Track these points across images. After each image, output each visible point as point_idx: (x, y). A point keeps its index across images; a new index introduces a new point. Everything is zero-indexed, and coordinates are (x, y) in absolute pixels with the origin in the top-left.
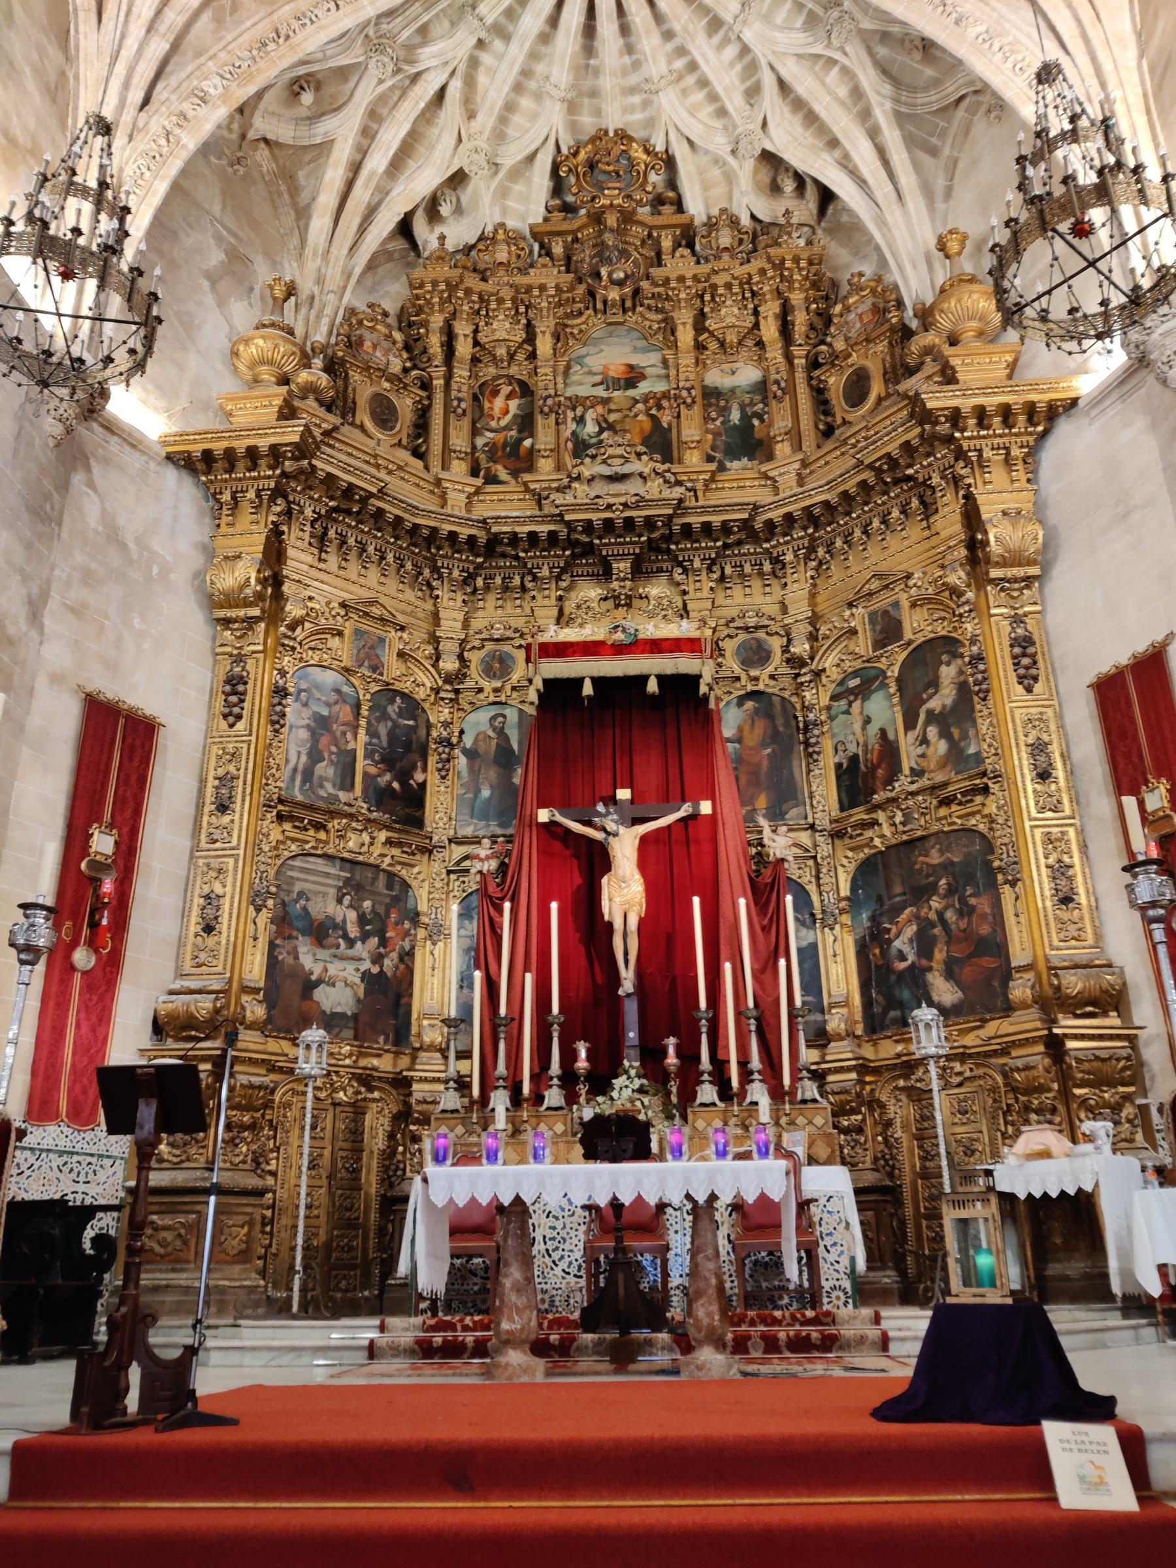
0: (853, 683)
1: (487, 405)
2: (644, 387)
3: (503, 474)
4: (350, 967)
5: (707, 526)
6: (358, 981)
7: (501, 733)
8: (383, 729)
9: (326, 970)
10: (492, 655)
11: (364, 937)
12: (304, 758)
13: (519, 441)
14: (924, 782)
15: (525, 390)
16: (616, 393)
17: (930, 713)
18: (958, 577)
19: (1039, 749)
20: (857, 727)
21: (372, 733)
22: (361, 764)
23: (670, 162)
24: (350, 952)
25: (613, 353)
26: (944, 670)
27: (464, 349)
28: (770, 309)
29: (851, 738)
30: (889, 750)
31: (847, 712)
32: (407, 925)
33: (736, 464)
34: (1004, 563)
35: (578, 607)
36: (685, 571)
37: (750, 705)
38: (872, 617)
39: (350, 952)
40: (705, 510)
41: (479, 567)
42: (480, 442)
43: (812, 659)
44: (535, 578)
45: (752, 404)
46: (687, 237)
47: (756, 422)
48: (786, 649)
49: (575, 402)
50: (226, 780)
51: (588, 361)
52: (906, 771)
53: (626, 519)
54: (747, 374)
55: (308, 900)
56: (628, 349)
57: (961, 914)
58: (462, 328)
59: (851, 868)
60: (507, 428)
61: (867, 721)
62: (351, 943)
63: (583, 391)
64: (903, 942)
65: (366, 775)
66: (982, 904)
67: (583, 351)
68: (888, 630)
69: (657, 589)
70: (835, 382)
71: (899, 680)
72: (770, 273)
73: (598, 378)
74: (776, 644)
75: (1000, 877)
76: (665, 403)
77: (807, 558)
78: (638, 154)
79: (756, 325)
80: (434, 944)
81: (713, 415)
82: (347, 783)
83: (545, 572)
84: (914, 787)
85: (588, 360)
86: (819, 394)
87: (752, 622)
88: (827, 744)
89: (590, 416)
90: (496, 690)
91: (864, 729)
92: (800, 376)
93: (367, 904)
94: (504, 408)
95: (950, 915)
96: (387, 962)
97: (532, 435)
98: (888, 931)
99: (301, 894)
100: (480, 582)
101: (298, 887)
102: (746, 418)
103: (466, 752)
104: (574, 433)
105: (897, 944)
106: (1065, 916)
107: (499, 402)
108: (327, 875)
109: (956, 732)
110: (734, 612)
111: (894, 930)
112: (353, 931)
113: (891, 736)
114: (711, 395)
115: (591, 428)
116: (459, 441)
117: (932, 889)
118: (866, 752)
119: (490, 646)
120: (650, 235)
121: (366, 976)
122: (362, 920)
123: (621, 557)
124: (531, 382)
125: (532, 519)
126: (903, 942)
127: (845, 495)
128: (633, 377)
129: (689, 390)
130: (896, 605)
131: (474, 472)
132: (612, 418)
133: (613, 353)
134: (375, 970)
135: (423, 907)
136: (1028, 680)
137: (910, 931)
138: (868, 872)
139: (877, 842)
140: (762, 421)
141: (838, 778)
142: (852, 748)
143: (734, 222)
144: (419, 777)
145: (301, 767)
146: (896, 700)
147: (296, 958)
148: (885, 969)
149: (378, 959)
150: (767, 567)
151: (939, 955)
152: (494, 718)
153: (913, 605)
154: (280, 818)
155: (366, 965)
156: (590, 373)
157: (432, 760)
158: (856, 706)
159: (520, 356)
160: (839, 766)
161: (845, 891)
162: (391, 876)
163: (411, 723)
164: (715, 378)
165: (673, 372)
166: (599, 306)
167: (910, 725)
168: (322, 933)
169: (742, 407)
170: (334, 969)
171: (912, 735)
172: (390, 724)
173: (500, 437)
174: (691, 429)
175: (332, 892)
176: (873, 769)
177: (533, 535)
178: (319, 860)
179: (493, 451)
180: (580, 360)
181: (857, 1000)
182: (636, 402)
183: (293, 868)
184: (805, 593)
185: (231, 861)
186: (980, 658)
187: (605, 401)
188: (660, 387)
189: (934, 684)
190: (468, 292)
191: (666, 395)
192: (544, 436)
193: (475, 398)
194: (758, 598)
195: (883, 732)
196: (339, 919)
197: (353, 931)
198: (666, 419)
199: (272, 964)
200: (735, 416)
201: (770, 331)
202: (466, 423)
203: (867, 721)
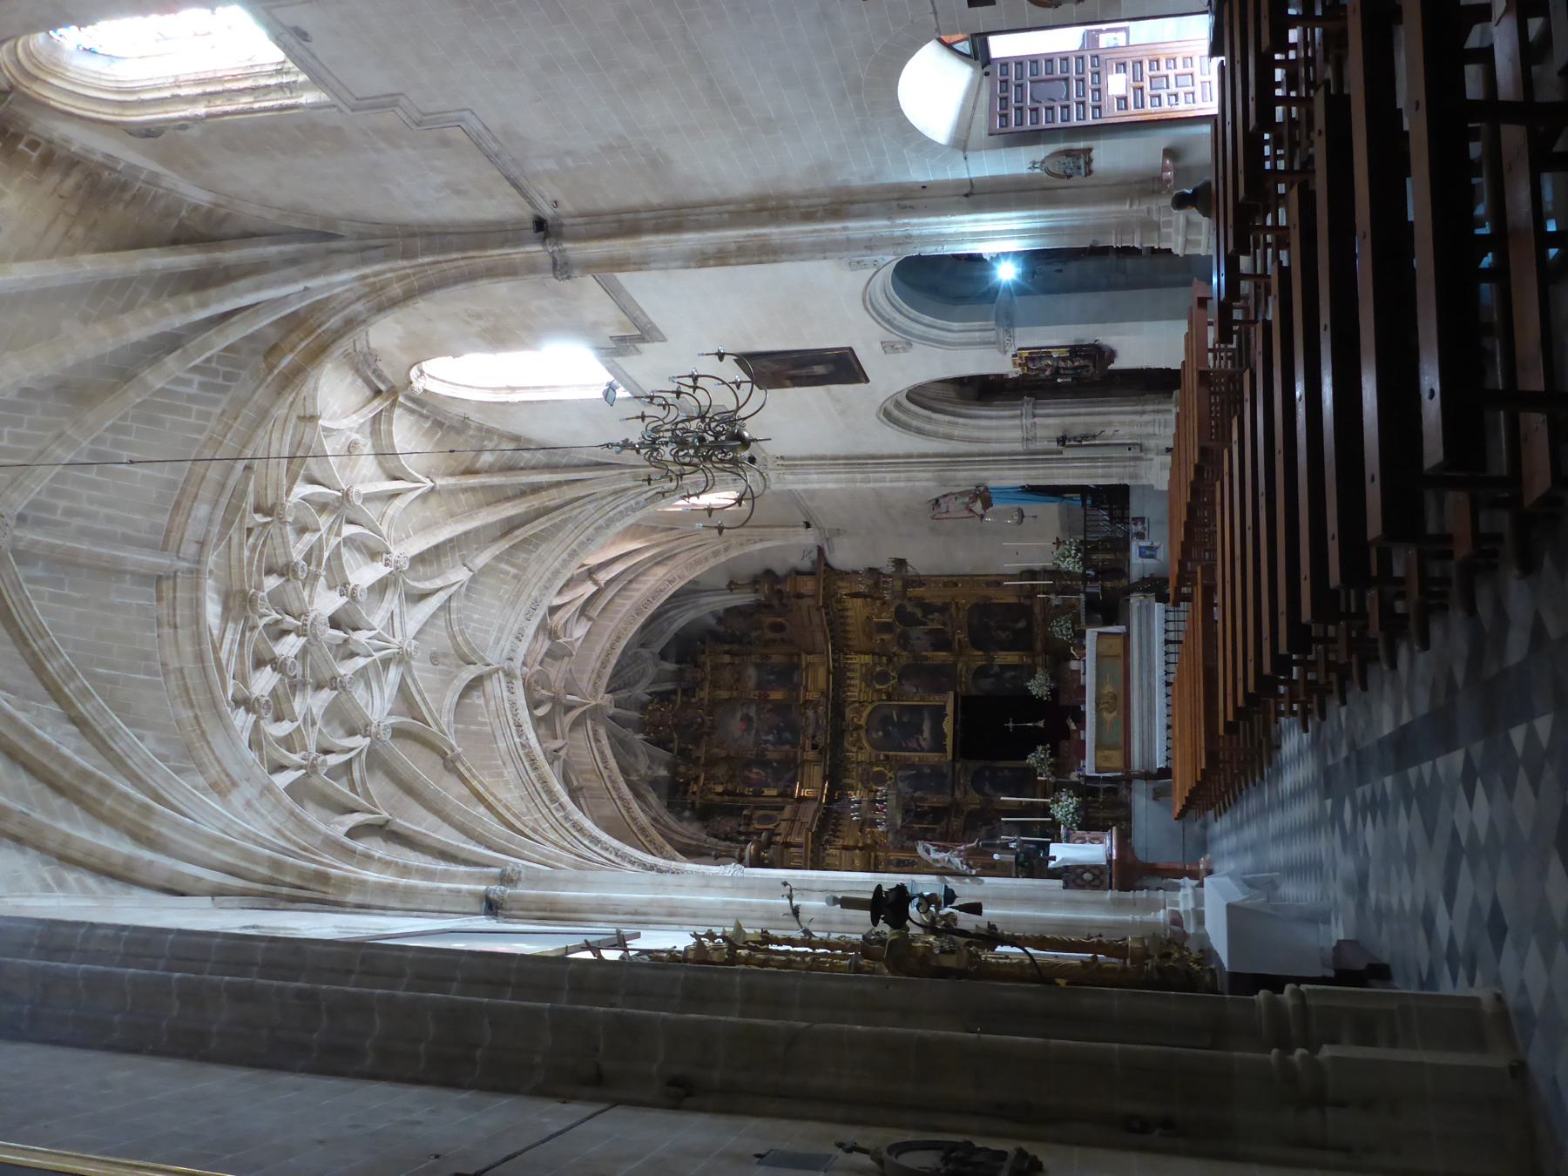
2: (752, 712)
15: (748, 765)
18: (878, 603)
25: (735, 725)
27: (730, 787)
28: (727, 659)
30: (931, 632)
33: (796, 679)
54: (751, 674)
58: (720, 789)
63: (751, 739)
64: (1003, 635)
68: (886, 628)
70: (770, 635)
94: (755, 773)
114: (761, 685)
115: (770, 738)
126: (1003, 635)
128: (747, 719)
133: (735, 725)
138: (976, 643)
174: (776, 695)
198: (770, 706)
201: (737, 660)
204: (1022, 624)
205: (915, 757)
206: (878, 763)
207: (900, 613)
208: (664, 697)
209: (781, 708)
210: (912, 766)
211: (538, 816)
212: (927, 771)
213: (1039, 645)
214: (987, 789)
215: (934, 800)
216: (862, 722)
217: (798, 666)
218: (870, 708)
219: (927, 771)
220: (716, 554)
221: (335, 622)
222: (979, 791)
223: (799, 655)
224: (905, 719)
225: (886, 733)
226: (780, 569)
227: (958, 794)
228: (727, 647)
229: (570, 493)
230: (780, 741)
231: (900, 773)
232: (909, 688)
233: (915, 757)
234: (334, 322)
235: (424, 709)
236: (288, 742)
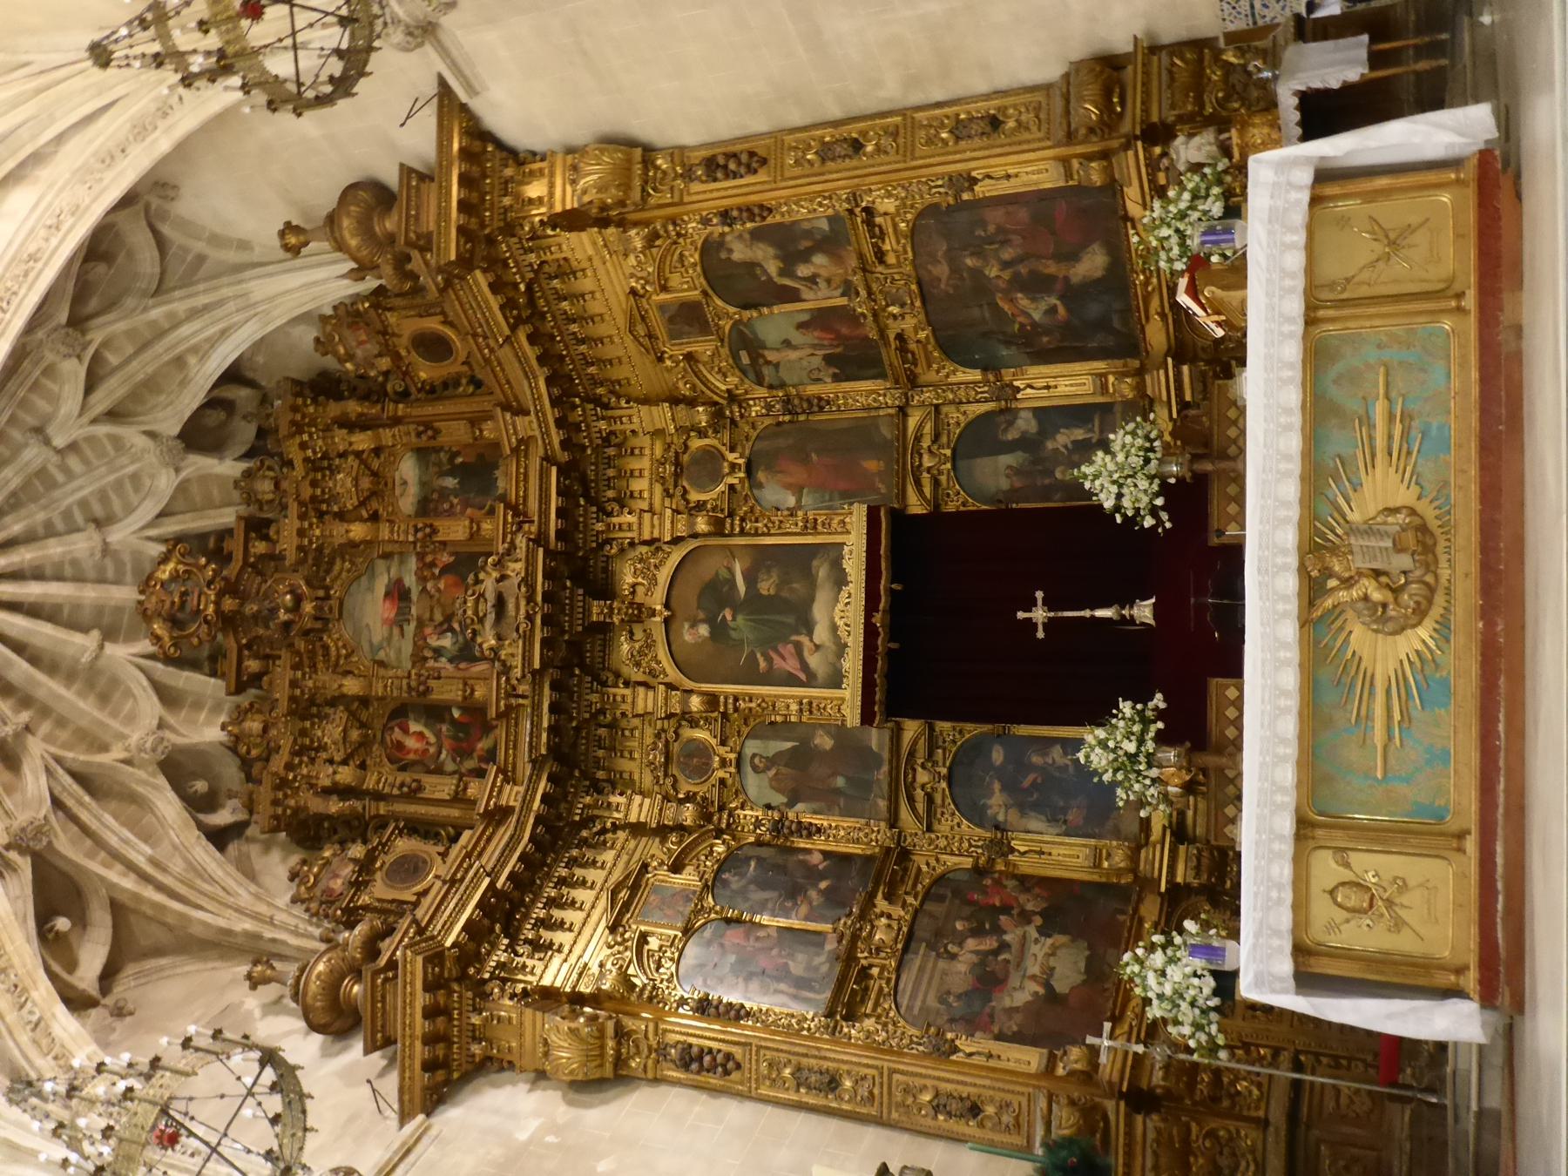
0: (745, 359)
1: (411, 756)
2: (410, 581)
4: (1035, 949)
5: (560, 513)
6: (1049, 941)
7: (771, 761)
8: (758, 895)
9: (1033, 977)
10: (684, 768)
11: (998, 930)
12: (782, 986)
13: (453, 721)
14: (857, 279)
15: (400, 713)
16: (414, 611)
17: (783, 273)
20: (793, 355)
21: (761, 908)
22: (796, 923)
23: (178, 539)
24: (1015, 947)
25: (371, 611)
26: (736, 256)
28: (340, 438)
29: (805, 363)
30: (821, 320)
31: (777, 366)
32: (988, 882)
33: (501, 484)
34: (626, 186)
35: (638, 665)
36: (609, 541)
37: (761, 476)
38: (673, 335)
39: (1015, 947)
40: (544, 513)
41: (584, 775)
42: (450, 767)
43: (716, 403)
44: (602, 711)
45: (439, 464)
46: (257, 526)
47: (459, 460)
48: (702, 434)
49: (418, 659)
51: (377, 638)
52: (843, 301)
53: (544, 600)
54: (408, 469)
55: (949, 993)
56: (369, 597)
57: (1005, 242)
59: (950, 366)
60: (438, 735)
61: (787, 344)
62: (1004, 946)
63: (407, 648)
64: (1035, 310)
65: (806, 919)
66: (996, 217)
67: (366, 647)
68: (689, 317)
69: (627, 576)
70: (425, 372)
71: (745, 307)
72: (305, 437)
73: (396, 631)
74: (696, 443)
75: (966, 196)
76: (429, 559)
77: (606, 407)
78: (165, 573)
79: (358, 454)
80: (1012, 850)
81: (446, 506)
83: (594, 698)
84: (863, 293)
85: (376, 639)
86: (433, 392)
87: (670, 469)
88: (812, 390)
89: (434, 642)
90: (724, 763)
91: (795, 348)
92: (417, 411)
93: (959, 926)
94: (416, 736)
95: (1007, 254)
96: (1030, 907)
97: (449, 709)
98: (1022, 326)
99: (942, 1000)
100: (601, 774)
101: (932, 1002)
102: (451, 473)
103: (791, 804)
104: (450, 661)
105: (1037, 316)
106: (1011, 124)
107: (411, 743)
108: (921, 969)
109: (805, 244)
110: (658, 489)
111: (1021, 319)
112: (990, 943)
113: (805, 317)
114: (426, 507)
115: (447, 642)
117: (977, 273)
118: (821, 347)
119: (674, 770)
120: (253, 566)
121: (1044, 931)
122: (977, 932)
123: (587, 611)
124: (392, 706)
125: (536, 707)
126: (1035, 310)
127: (541, 360)
128: (398, 593)
129: (417, 530)
130: (662, 307)
131: (480, 774)
132: (438, 617)
134: (1038, 921)
135: (967, 862)
137: (1023, 301)
138: (955, 348)
139: (922, 335)
140: (458, 454)
141: (848, 379)
142: (817, 361)
143: (248, 474)
144: (816, 858)
145: (792, 990)
146: (765, 310)
147: (1017, 1009)
148: (1067, 329)
149: (1025, 917)
150: (611, 451)
151: (1051, 268)
152: (755, 769)
153: (664, 288)
154: (850, 1017)
155: (1032, 932)
156: (389, 639)
157: (802, 843)
158: (771, 356)
159: (364, 716)
160: (837, 378)
161: (975, 375)
162: (927, 895)
163: (753, 864)
164: (407, 503)
165: (396, 548)
166: (318, 625)
167: (792, 296)
168: (989, 980)
169: (442, 474)
170: (1035, 969)
171: (806, 293)
172: (752, 887)
173: (447, 743)
174: (455, 530)
175: (942, 964)
176: (839, 336)
177: (553, 709)
178: (904, 977)
179: (462, 752)
180: (374, 649)
181: (1100, 366)
182: (424, 589)
183: (910, 1008)
184: (644, 409)
185: (896, 1077)
186: (726, 216)
187: (421, 624)
188: (413, 563)
189: (751, 266)
190: (289, 767)
191: (421, 557)
192: (447, 692)
193: (403, 769)
194: (645, 463)
195: (801, 326)
196: (974, 958)
197: (990, 943)
198: (446, 558)
199: (1018, 1038)
200: (450, 482)
201: (362, 441)
202: (428, 780)
203: (787, 344)
204: (1093, 263)
205: (788, 699)
207: (719, 271)
208: (212, 546)
212: (824, 742)
213: (1156, 335)
214: (997, 803)
219: (824, 742)
220: (141, 130)
222: (976, 815)
224: (766, 587)
225: (719, 631)
231: (752, 747)
232: (775, 494)
233: (788, 699)
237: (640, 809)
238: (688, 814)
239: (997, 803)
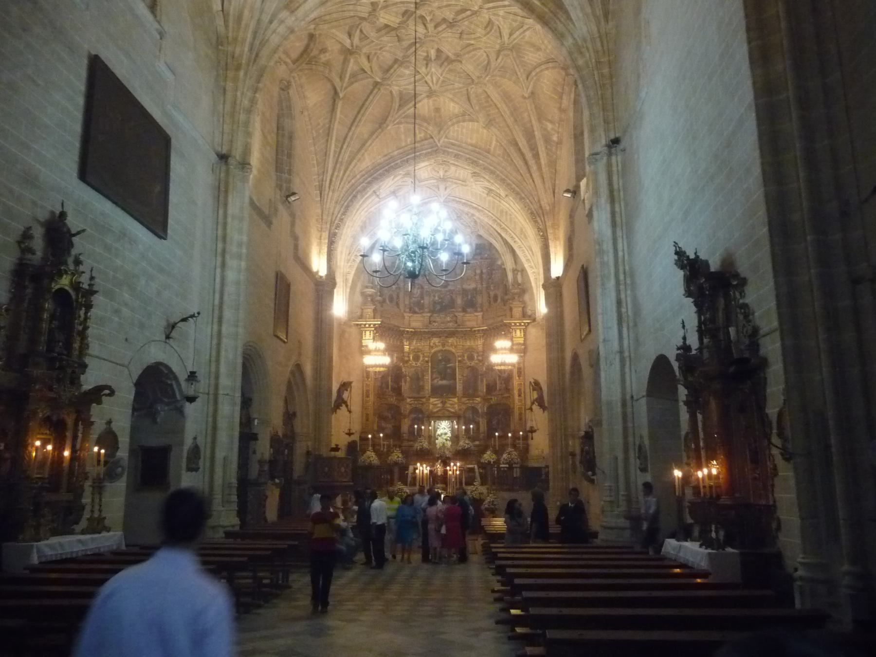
2: (450, 288)
3: (417, 310)
19: (520, 390)
28: (478, 272)
33: (469, 310)
50: (368, 391)
54: (473, 286)
69: (450, 340)
82: (388, 388)
114: (465, 292)
116: (407, 302)
126: (494, 423)
136: (519, 376)
138: (490, 407)
164: (465, 286)
168: (385, 419)
174: (459, 301)
198: (454, 297)
199: (378, 426)
201: (477, 277)
205: (428, 377)
206: (424, 356)
209: (452, 304)
210: (423, 376)
211: (358, 176)
212: (421, 383)
214: (413, 416)
215: (405, 387)
216: (447, 348)
217: (476, 311)
218: (453, 350)
219: (421, 383)
221: (439, 51)
222: (411, 412)
223: (482, 311)
226: (526, 297)
227: (408, 400)
228: (484, 271)
229: (536, 175)
230: (435, 303)
232: (466, 372)
233: (428, 377)
234: (560, 27)
235: (405, 109)
236: (364, 37)
237: (407, 348)
238: (406, 359)
239: (413, 416)
